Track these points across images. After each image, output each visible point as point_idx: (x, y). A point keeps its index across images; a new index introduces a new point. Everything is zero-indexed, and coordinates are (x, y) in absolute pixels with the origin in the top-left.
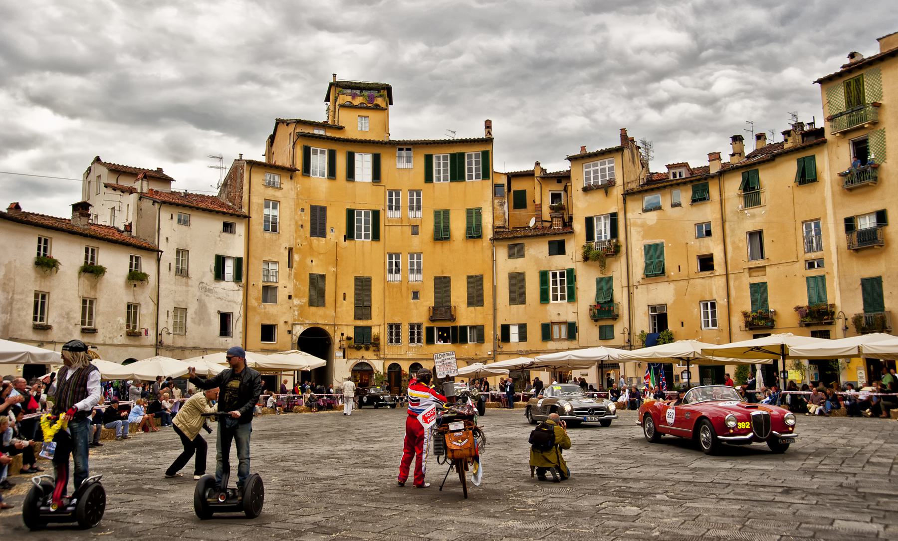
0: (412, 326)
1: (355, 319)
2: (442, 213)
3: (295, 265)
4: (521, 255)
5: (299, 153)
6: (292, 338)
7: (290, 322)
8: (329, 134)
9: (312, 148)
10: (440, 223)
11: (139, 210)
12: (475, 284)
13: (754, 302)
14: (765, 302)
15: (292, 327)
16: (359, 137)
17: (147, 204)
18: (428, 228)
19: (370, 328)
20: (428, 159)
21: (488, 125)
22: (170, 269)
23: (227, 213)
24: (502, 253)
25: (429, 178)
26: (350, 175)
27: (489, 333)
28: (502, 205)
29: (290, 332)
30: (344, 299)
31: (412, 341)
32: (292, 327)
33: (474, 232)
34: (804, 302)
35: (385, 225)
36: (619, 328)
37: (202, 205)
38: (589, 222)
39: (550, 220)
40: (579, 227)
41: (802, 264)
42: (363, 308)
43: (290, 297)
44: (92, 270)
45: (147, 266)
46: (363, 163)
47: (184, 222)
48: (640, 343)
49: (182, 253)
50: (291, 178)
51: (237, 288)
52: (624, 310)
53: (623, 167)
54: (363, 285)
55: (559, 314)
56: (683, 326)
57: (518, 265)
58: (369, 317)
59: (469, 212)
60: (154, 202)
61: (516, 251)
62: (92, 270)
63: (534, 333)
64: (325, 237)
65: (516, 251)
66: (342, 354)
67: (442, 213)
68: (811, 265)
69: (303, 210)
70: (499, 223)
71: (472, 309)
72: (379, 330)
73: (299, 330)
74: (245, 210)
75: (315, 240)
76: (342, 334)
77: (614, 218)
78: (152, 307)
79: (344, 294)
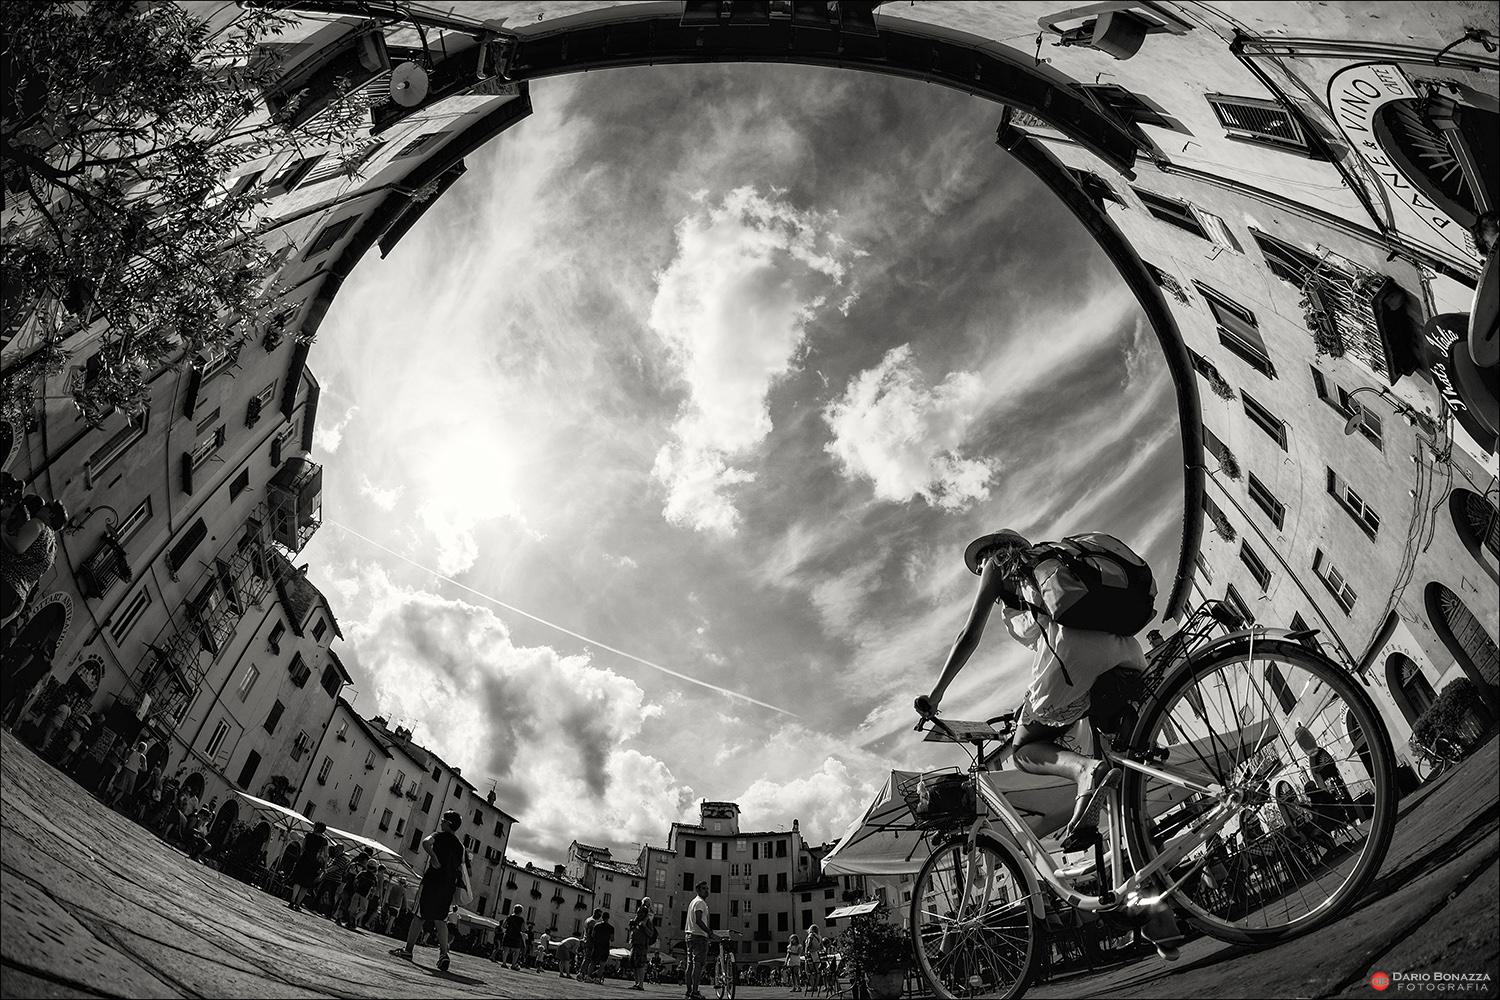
3: (673, 906)
12: (783, 917)
16: (715, 834)
18: (755, 884)
20: (755, 846)
21: (796, 822)
24: (798, 898)
25: (755, 856)
26: (709, 856)
28: (806, 869)
29: (669, 944)
45: (587, 900)
46: (717, 848)
57: (808, 906)
61: (806, 898)
65: (806, 898)
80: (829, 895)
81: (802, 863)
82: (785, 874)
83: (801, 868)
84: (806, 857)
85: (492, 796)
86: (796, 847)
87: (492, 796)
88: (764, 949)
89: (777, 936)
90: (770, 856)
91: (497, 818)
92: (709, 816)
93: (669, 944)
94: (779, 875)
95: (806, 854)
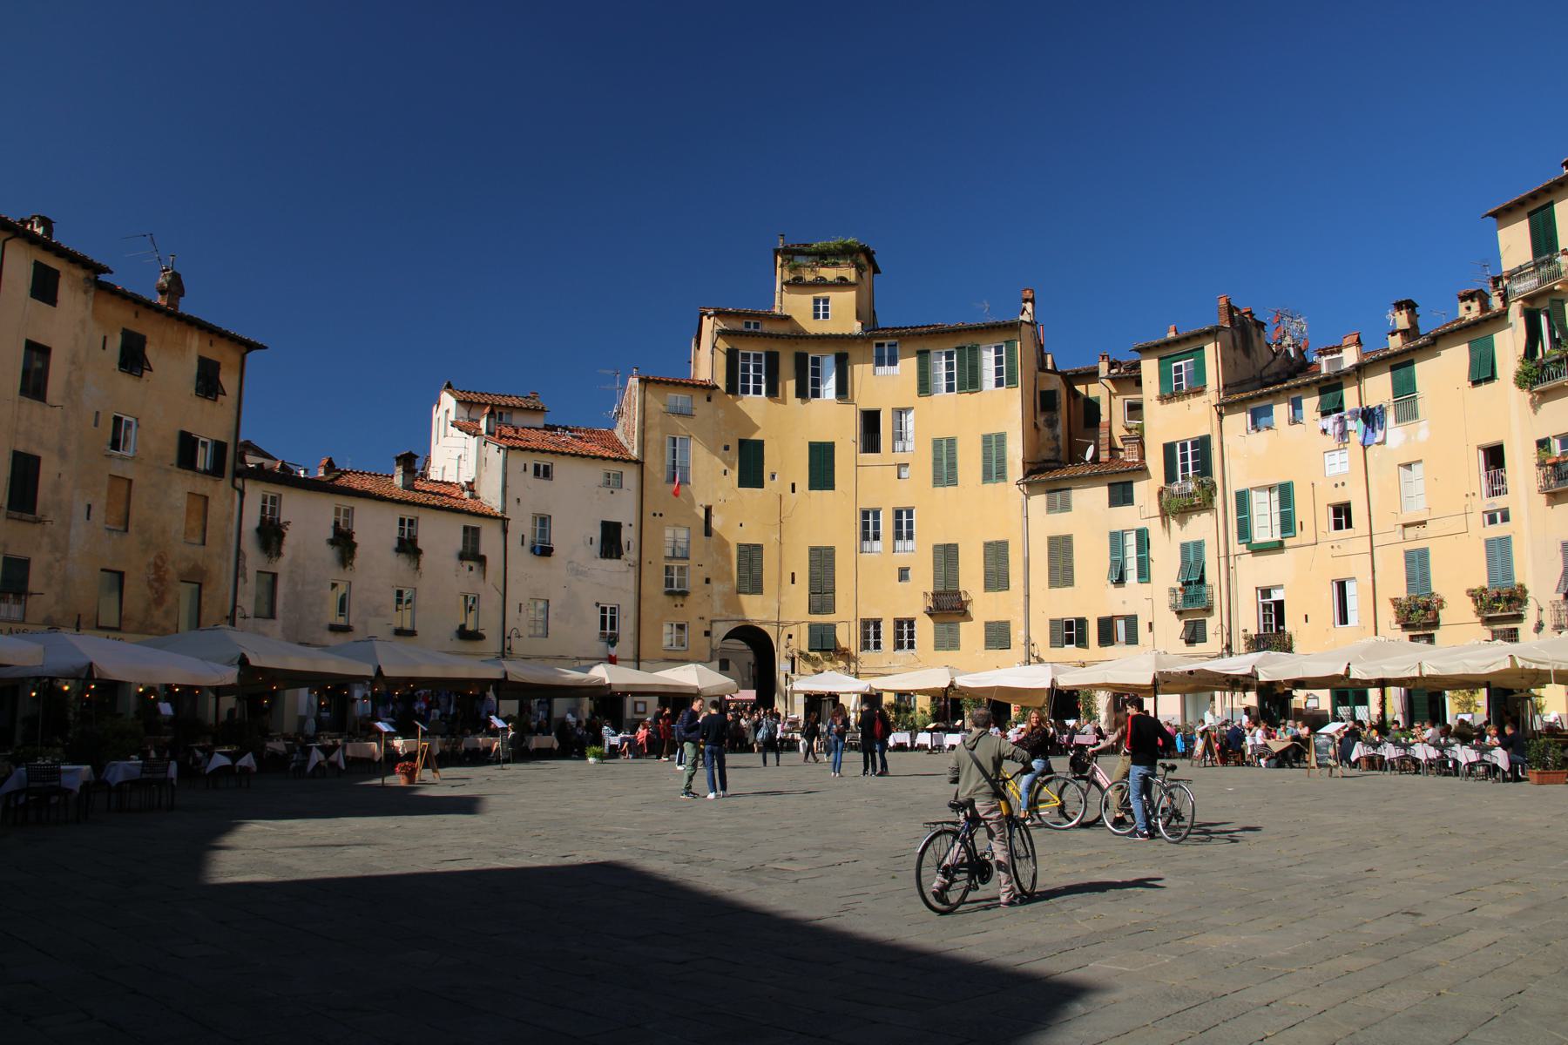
0: (899, 623)
1: (809, 612)
2: (945, 443)
4: (1066, 507)
5: (722, 360)
6: (711, 642)
7: (707, 620)
8: (766, 327)
9: (740, 351)
10: (942, 460)
11: (481, 462)
12: (996, 554)
13: (1410, 579)
14: (1425, 578)
15: (711, 625)
17: (492, 448)
18: (923, 466)
19: (832, 627)
22: (523, 544)
23: (609, 458)
24: (1039, 501)
25: (925, 387)
27: (1017, 636)
28: (1051, 424)
30: (793, 582)
31: (899, 646)
32: (711, 625)
33: (994, 470)
34: (1480, 580)
35: (857, 466)
36: (1212, 624)
39: (1122, 447)
40: (1155, 462)
41: (1477, 518)
42: (822, 594)
43: (708, 581)
44: (408, 547)
45: (490, 542)
47: (544, 472)
48: (1243, 649)
49: (544, 521)
50: (709, 399)
51: (625, 569)
52: (1218, 600)
53: (1217, 361)
54: (822, 560)
55: (1124, 602)
56: (1307, 621)
57: (1060, 524)
58: (829, 607)
59: (987, 440)
60: (500, 448)
62: (408, 547)
64: (763, 487)
66: (789, 666)
67: (945, 443)
68: (1492, 520)
69: (727, 448)
70: (1051, 455)
71: (991, 594)
73: (722, 629)
74: (635, 453)
75: (746, 491)
76: (790, 636)
77: (1202, 445)
78: (498, 598)
79: (793, 574)
81: (1043, 409)
82: (1001, 439)
84: (1053, 393)
85: (175, 287)
87: (175, 287)
88: (947, 641)
89: (984, 606)
91: (196, 345)
93: (707, 634)
94: (987, 440)
95: (1055, 383)
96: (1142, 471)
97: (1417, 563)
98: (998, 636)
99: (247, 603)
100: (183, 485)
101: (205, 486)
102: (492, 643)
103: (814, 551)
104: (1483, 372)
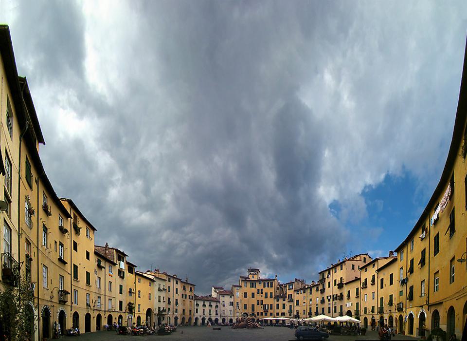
11: (217, 295)
20: (264, 283)
24: (276, 300)
25: (264, 287)
33: (271, 297)
37: (227, 293)
38: (289, 295)
42: (253, 310)
45: (218, 304)
47: (223, 297)
54: (253, 306)
61: (278, 301)
63: (280, 314)
65: (278, 301)
68: (317, 305)
72: (256, 314)
80: (284, 300)
83: (277, 291)
86: (276, 284)
88: (266, 314)
89: (270, 311)
90: (268, 287)
92: (251, 274)
96: (286, 297)
97: (310, 308)
98: (271, 314)
99: (195, 312)
100: (189, 300)
101: (191, 300)
102: (219, 315)
103: (252, 305)
104: (317, 290)
